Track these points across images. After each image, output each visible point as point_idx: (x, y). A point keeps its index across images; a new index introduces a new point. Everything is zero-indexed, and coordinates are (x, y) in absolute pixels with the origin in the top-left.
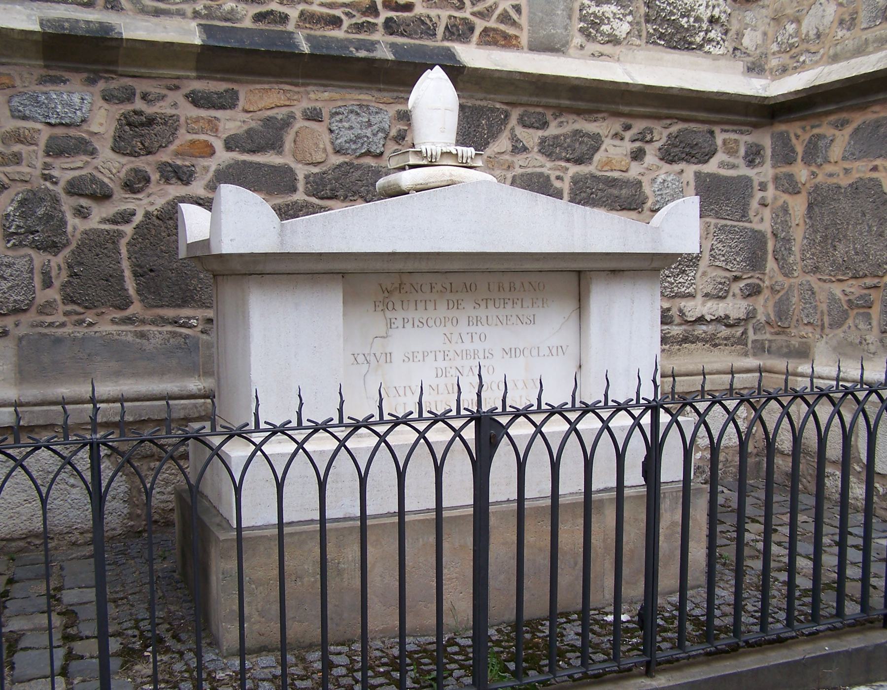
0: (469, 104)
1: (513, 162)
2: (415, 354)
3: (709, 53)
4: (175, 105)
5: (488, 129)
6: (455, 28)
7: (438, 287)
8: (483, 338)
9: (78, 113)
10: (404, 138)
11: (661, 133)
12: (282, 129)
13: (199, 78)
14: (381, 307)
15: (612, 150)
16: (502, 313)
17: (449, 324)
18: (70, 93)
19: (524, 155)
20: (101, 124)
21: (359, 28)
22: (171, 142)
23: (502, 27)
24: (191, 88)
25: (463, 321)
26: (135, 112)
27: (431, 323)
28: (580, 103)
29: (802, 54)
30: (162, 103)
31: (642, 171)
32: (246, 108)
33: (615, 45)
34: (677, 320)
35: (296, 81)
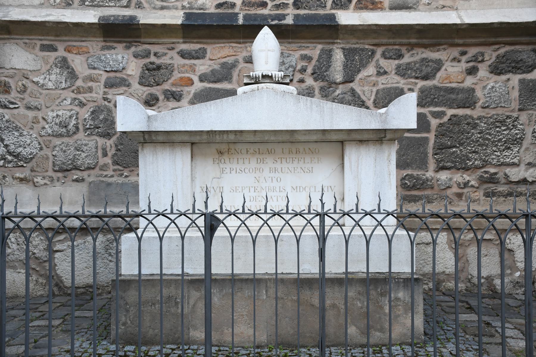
0: (347, 48)
1: (377, 81)
2: (237, 188)
4: (172, 58)
5: (360, 62)
7: (251, 151)
8: (279, 180)
9: (121, 65)
10: (305, 71)
11: (491, 55)
12: (231, 68)
13: (185, 42)
14: (217, 162)
15: (450, 69)
16: (290, 166)
17: (257, 172)
18: (117, 54)
19: (385, 76)
20: (133, 70)
22: (168, 79)
24: (181, 48)
25: (266, 171)
26: (152, 63)
27: (247, 171)
28: (424, 40)
30: (164, 58)
32: (211, 58)
34: (503, 181)
35: (239, 41)
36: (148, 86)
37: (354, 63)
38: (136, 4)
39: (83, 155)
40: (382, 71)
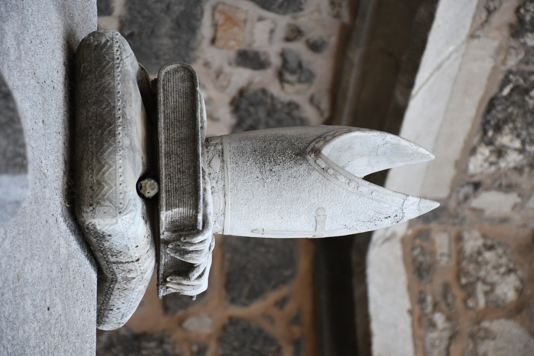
3: (473, 151)
29: (449, 319)
33: (511, 26)
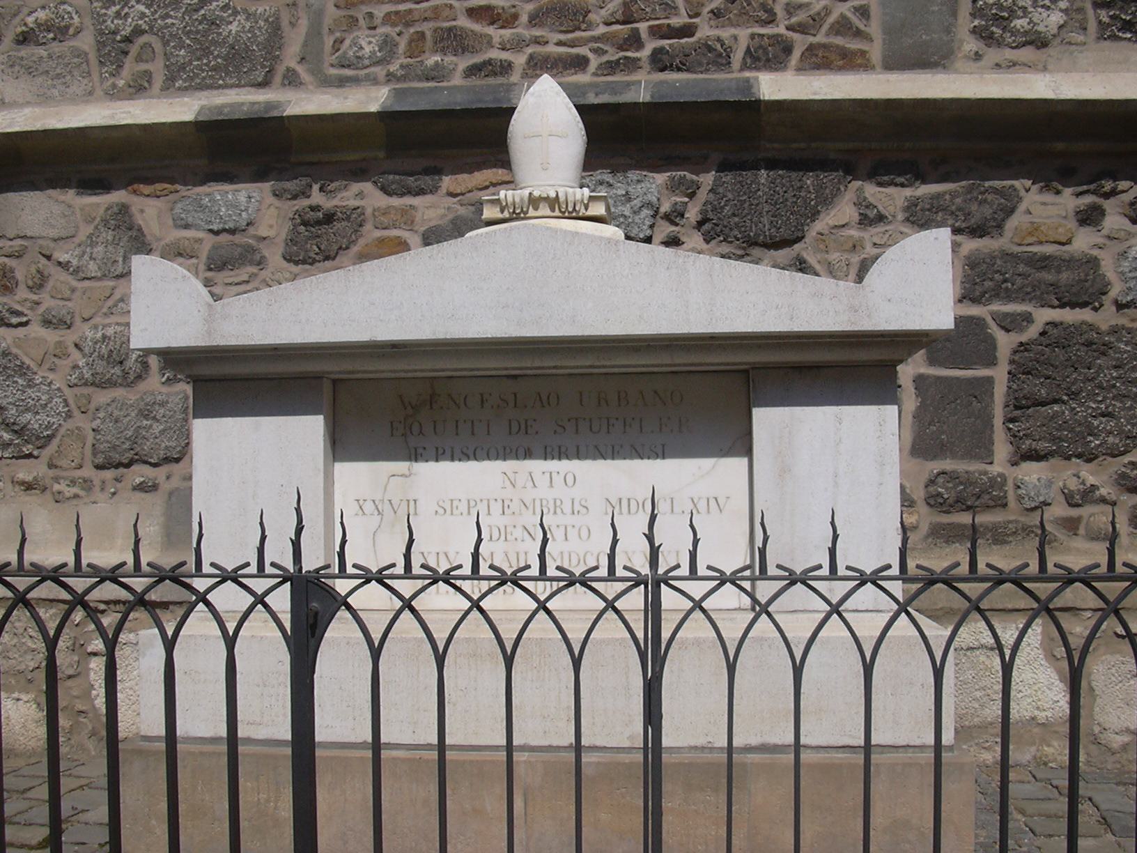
1: (861, 240)
2: (455, 503)
6: (761, 51)
9: (244, 215)
10: (682, 216)
19: (880, 228)
21: (612, 67)
23: (838, 41)
26: (314, 208)
31: (1100, 240)
32: (451, 190)
36: (304, 262)
37: (803, 194)
38: (285, 77)
39: (157, 428)
40: (872, 214)
